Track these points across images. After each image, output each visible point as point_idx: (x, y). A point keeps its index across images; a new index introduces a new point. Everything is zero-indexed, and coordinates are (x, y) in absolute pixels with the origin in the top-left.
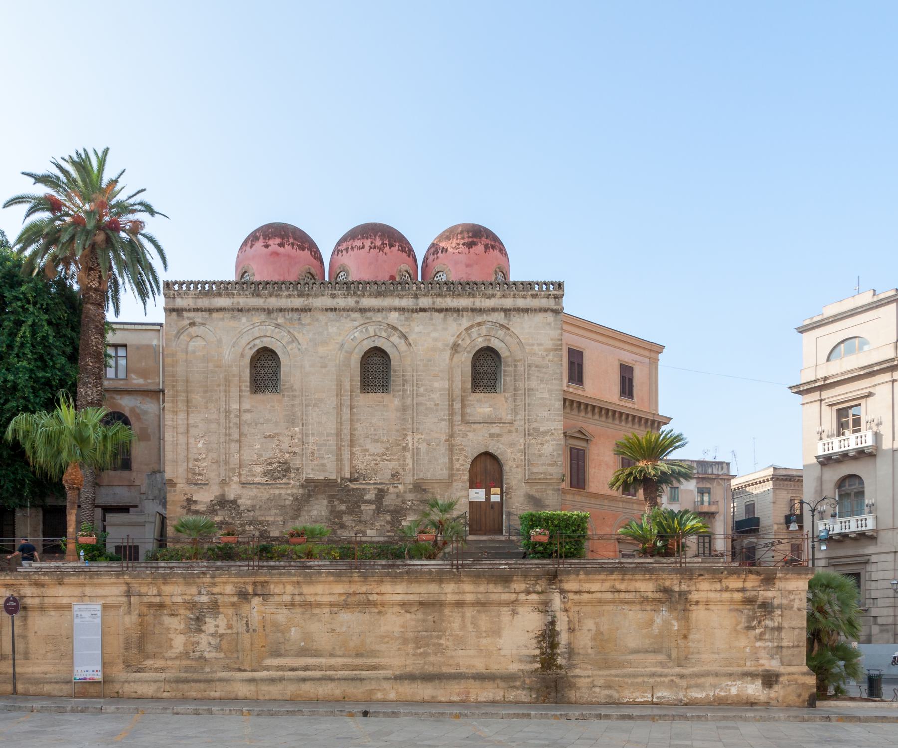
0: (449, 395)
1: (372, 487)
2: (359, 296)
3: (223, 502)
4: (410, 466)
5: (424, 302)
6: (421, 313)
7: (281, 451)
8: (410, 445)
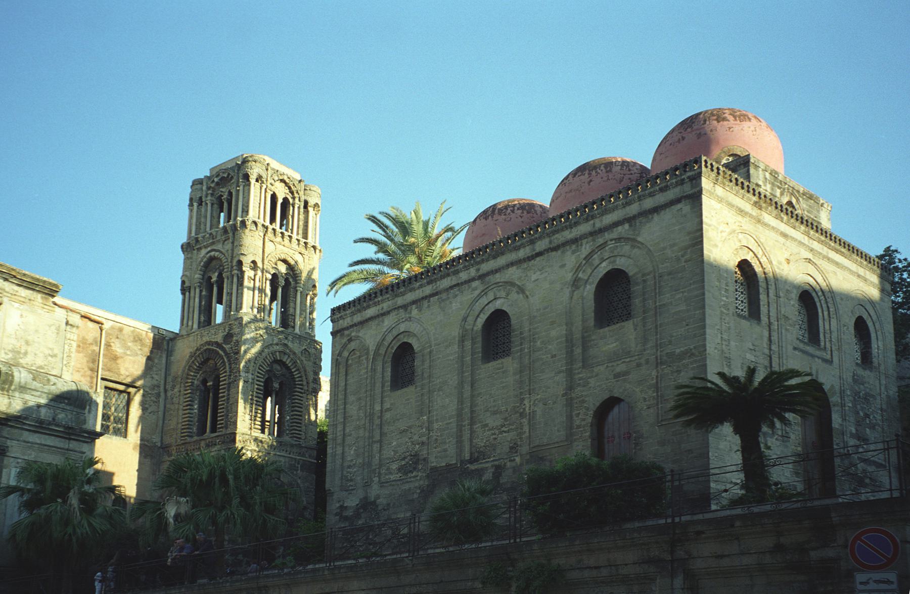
0: (567, 341)
1: (489, 465)
2: (479, 263)
3: (367, 505)
4: (527, 434)
5: (541, 245)
6: (538, 259)
7: (412, 442)
8: (527, 409)
